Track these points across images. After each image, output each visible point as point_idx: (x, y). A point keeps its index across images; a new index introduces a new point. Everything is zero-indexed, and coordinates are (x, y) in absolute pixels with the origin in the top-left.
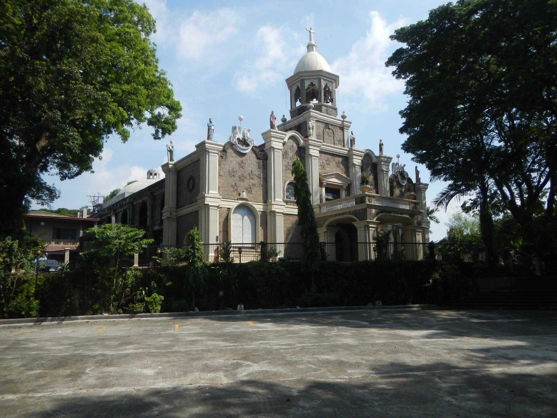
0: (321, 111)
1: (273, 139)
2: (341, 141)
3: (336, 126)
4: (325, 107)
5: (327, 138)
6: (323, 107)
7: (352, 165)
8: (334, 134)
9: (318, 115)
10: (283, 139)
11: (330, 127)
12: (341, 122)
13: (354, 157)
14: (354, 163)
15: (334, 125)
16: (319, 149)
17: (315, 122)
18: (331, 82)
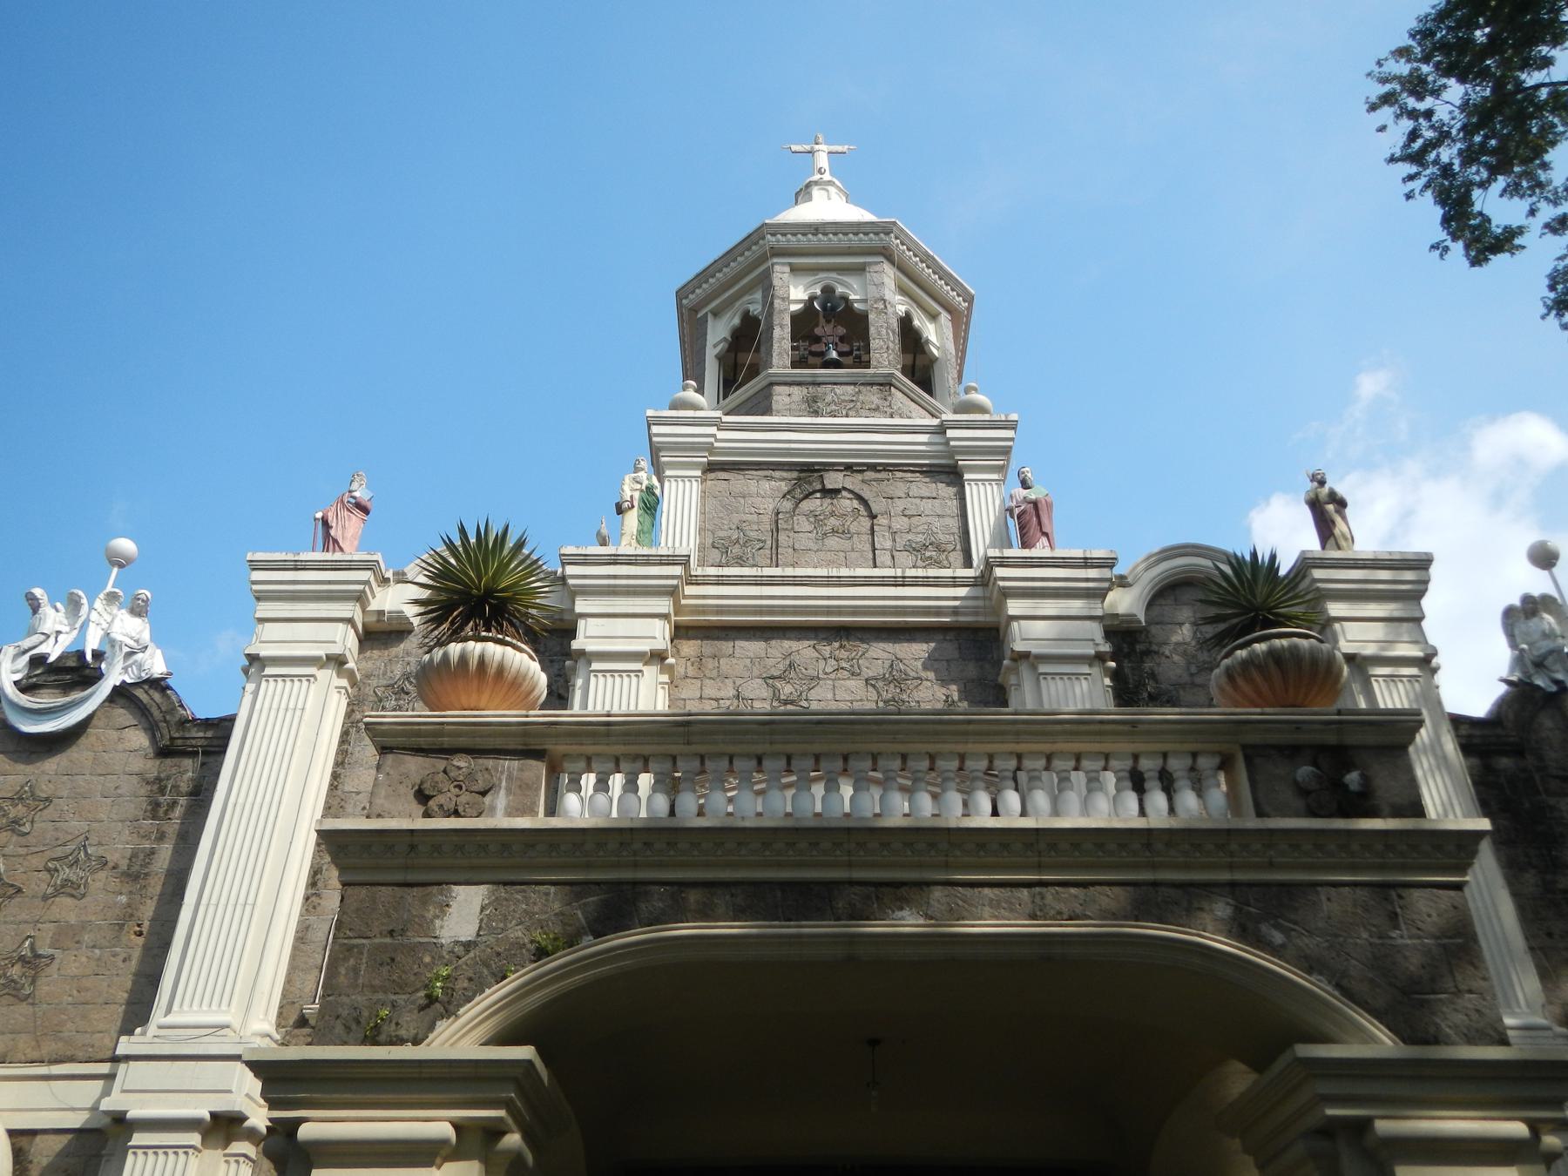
0: (767, 411)
1: (266, 609)
2: (939, 548)
3: (886, 468)
4: (796, 390)
5: (811, 545)
6: (777, 389)
7: (1016, 671)
8: (873, 517)
9: (713, 430)
10: (360, 598)
11: (833, 480)
12: (924, 438)
13: (1011, 612)
14: (1019, 646)
15: (873, 467)
16: (663, 605)
17: (699, 473)
18: (860, 270)
